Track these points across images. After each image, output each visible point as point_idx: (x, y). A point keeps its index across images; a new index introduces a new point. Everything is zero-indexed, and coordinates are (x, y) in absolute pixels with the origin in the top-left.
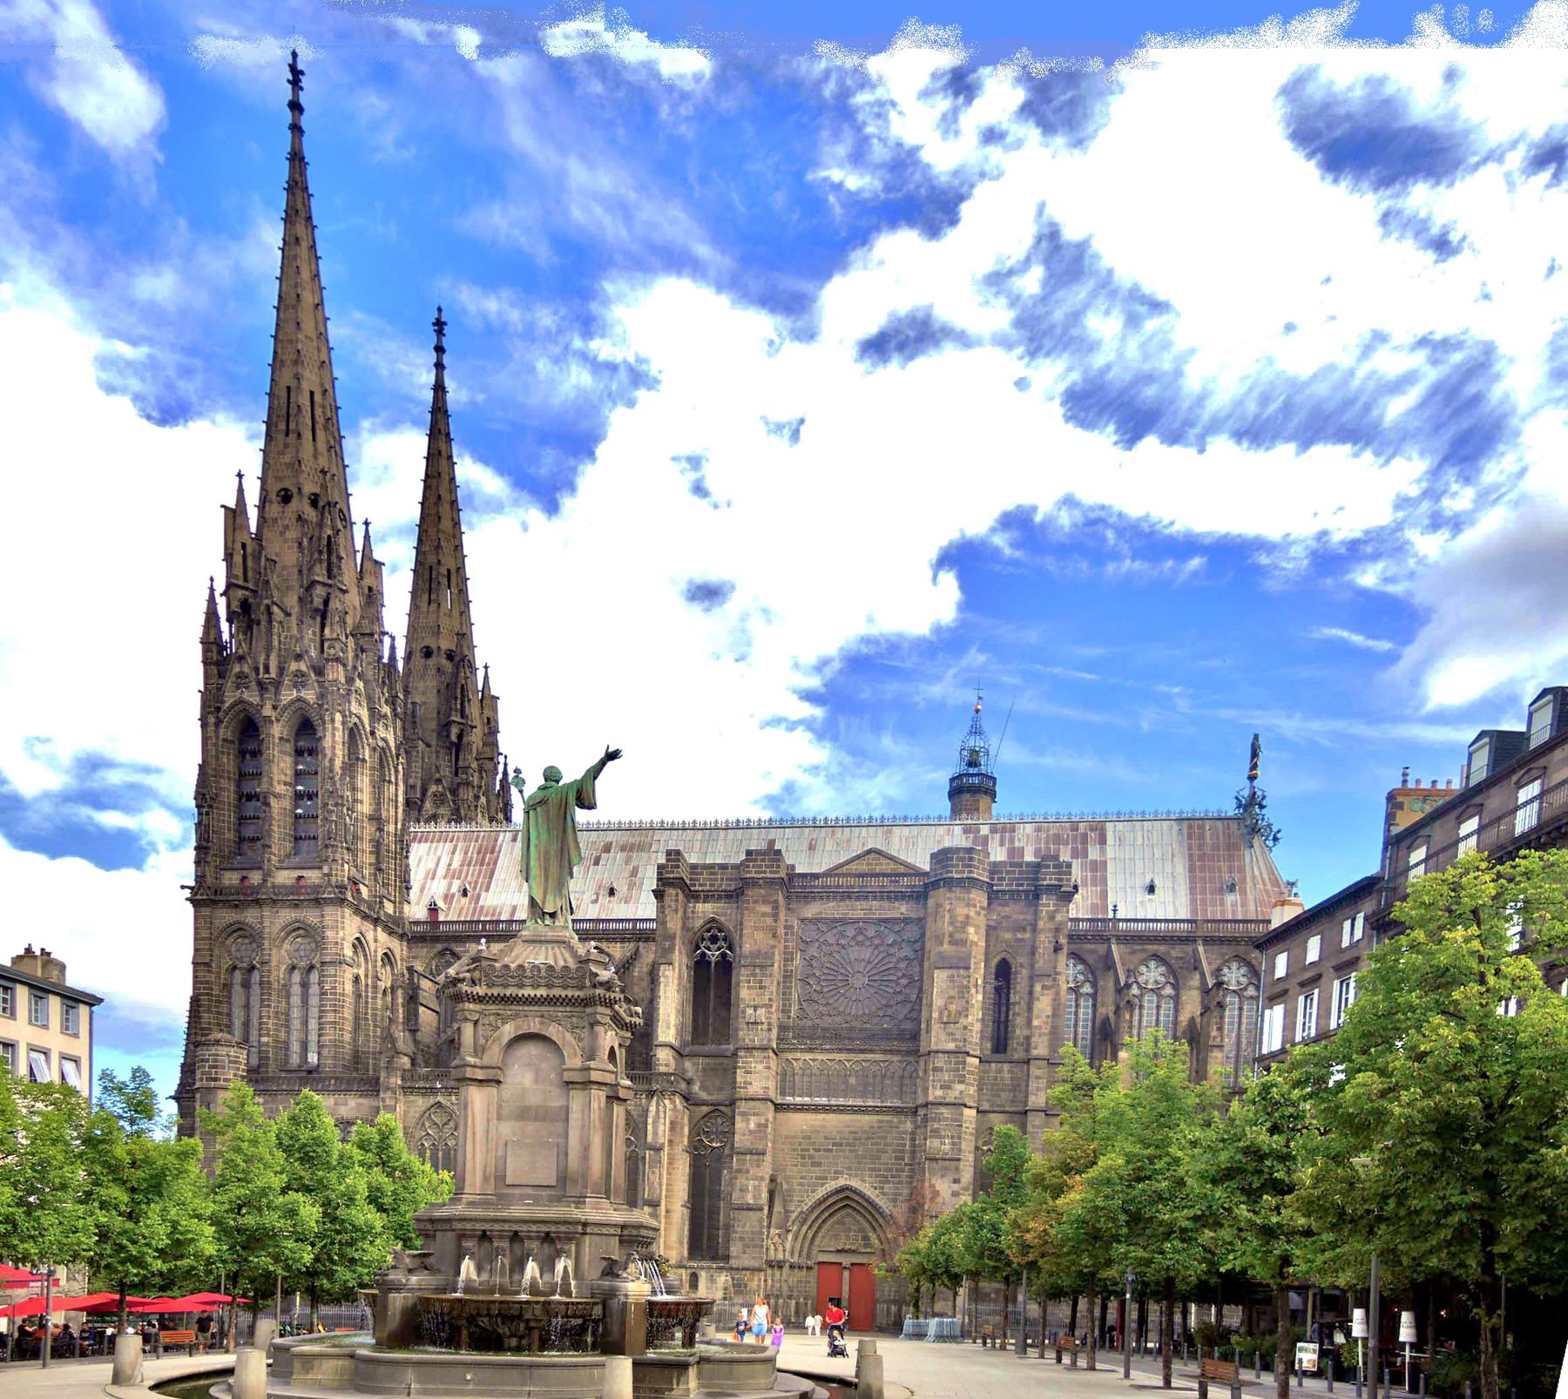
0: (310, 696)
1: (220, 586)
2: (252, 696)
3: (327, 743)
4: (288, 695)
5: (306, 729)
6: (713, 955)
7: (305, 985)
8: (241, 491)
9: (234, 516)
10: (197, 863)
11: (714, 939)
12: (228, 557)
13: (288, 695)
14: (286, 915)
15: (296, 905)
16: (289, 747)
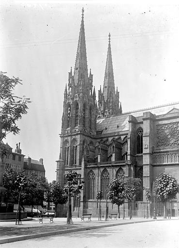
0: (77, 99)
1: (67, 85)
2: (70, 101)
3: (80, 107)
4: (75, 99)
5: (78, 104)
6: (140, 135)
7: (76, 150)
8: (71, 71)
9: (70, 74)
10: (62, 130)
11: (140, 132)
12: (69, 80)
13: (75, 99)
14: (74, 137)
15: (74, 135)
16: (75, 108)
